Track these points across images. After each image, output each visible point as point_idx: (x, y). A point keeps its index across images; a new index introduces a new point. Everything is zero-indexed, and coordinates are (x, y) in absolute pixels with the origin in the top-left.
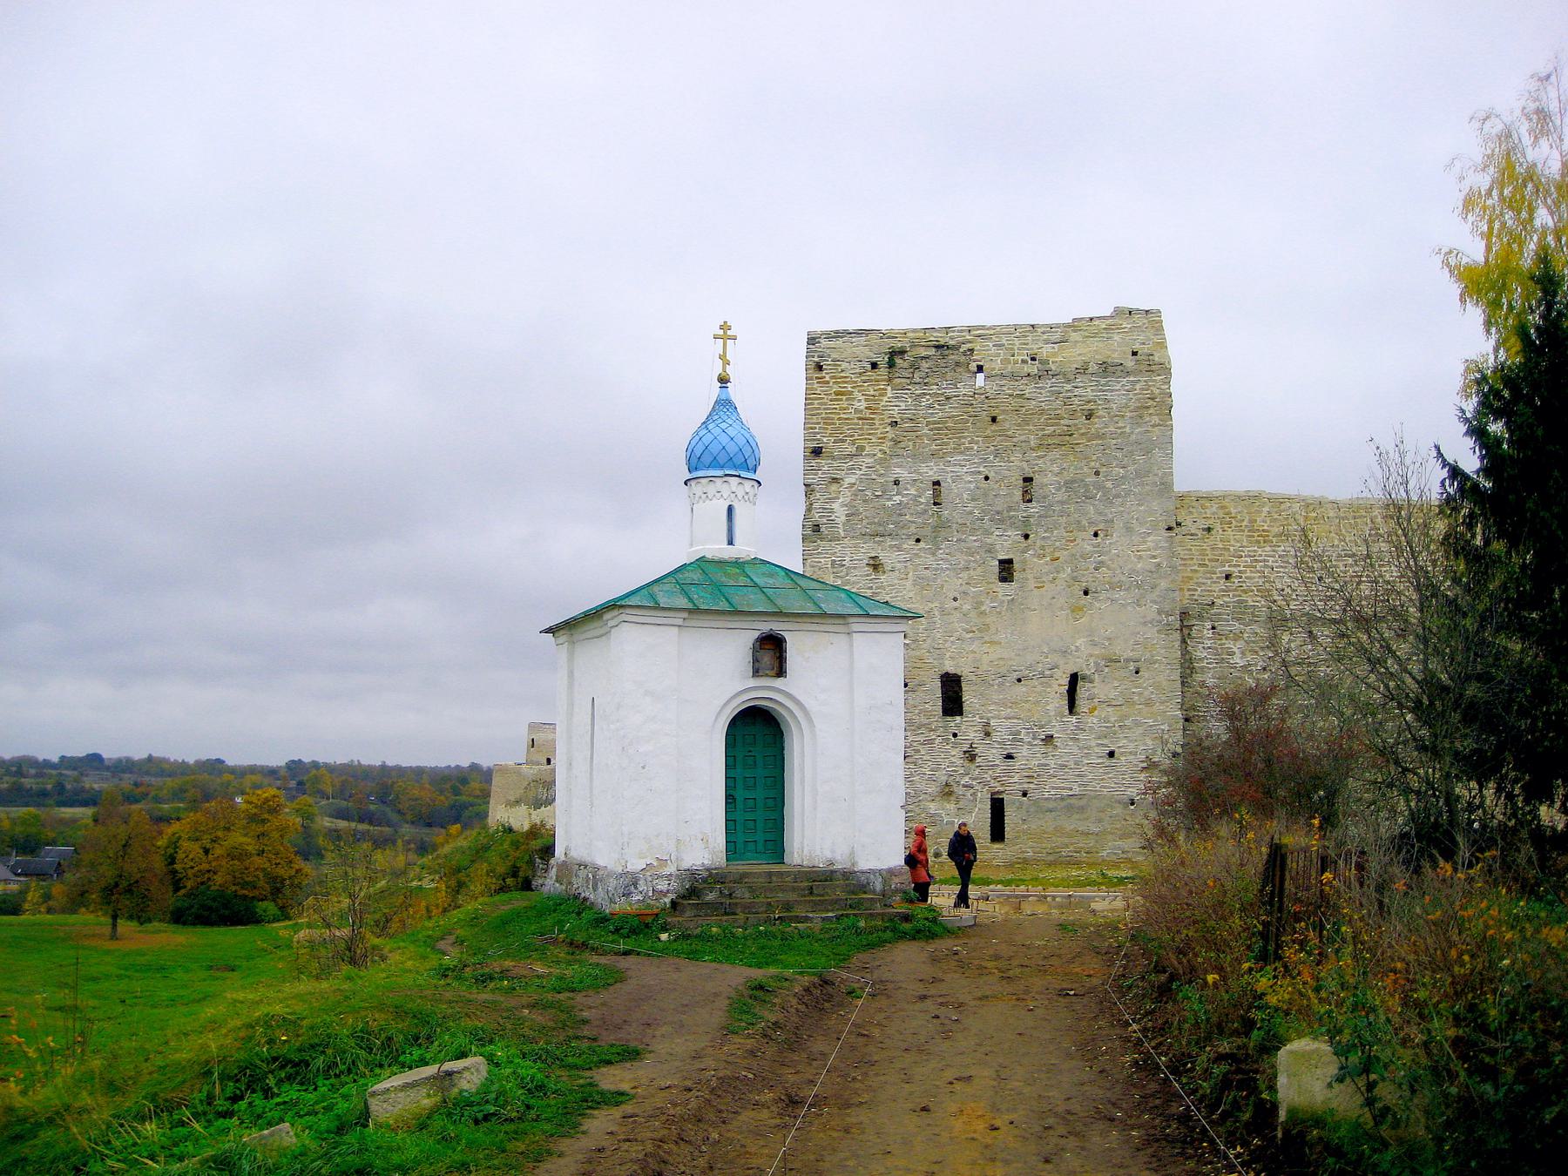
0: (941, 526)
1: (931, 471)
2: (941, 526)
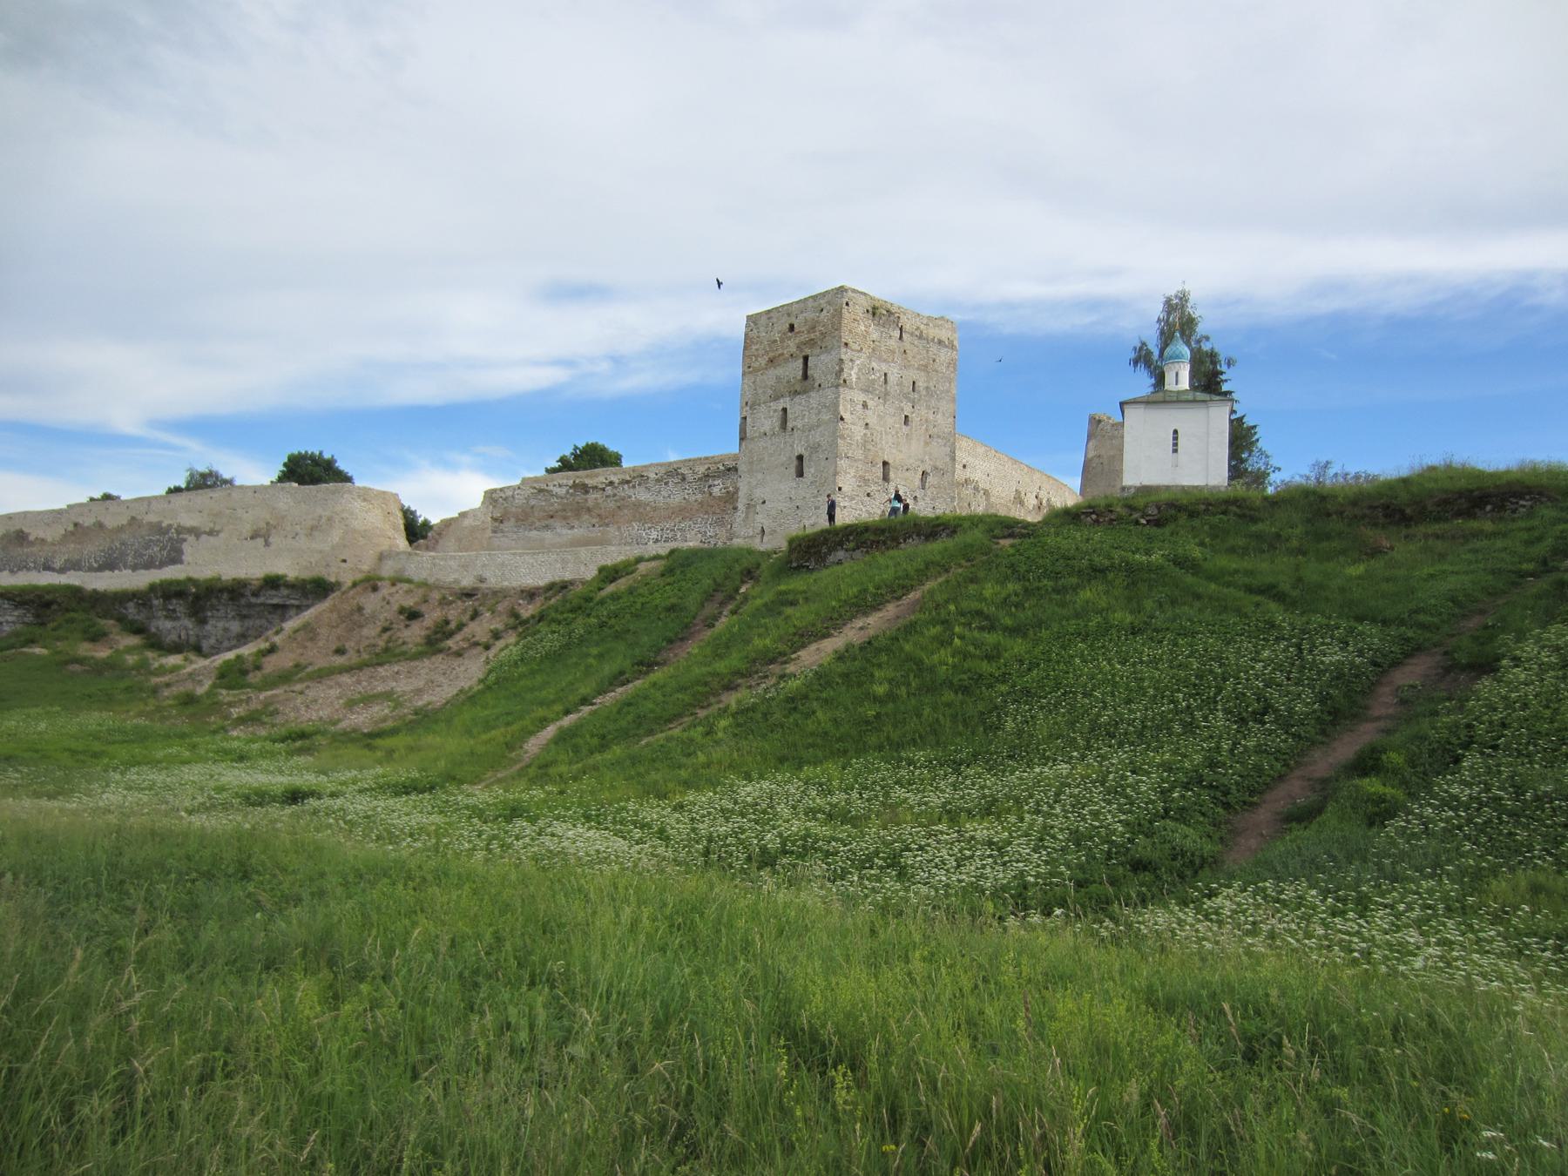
0: (887, 394)
1: (884, 367)
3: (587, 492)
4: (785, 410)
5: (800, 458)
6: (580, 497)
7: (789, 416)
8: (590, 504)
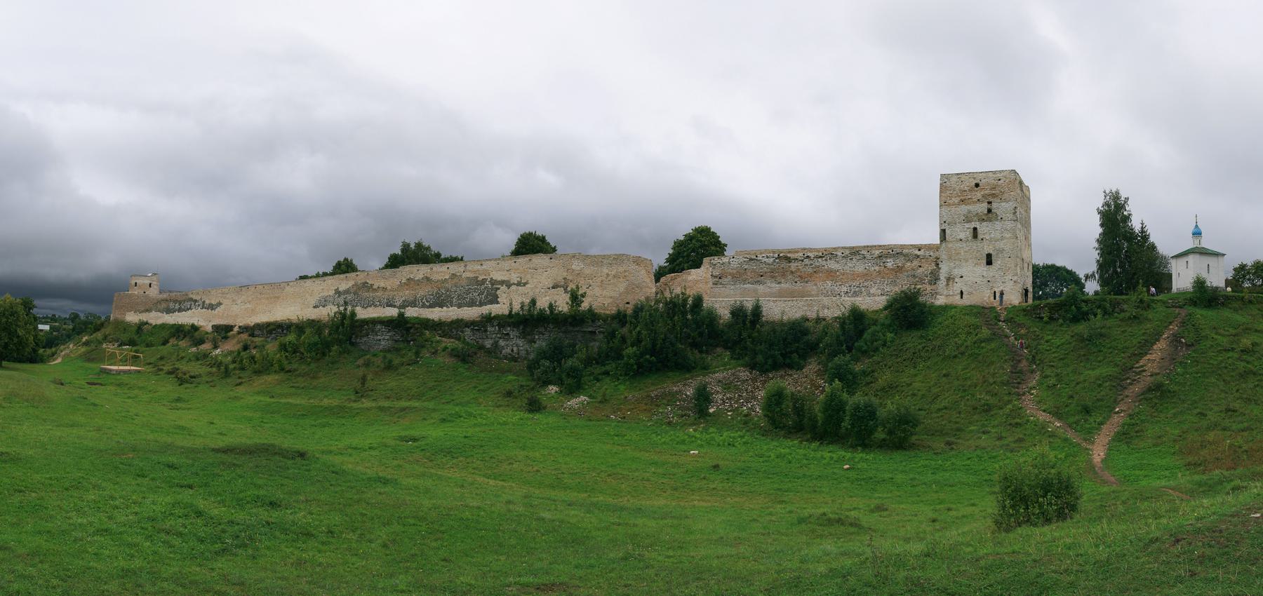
4: (975, 229)
5: (989, 256)
6: (784, 264)
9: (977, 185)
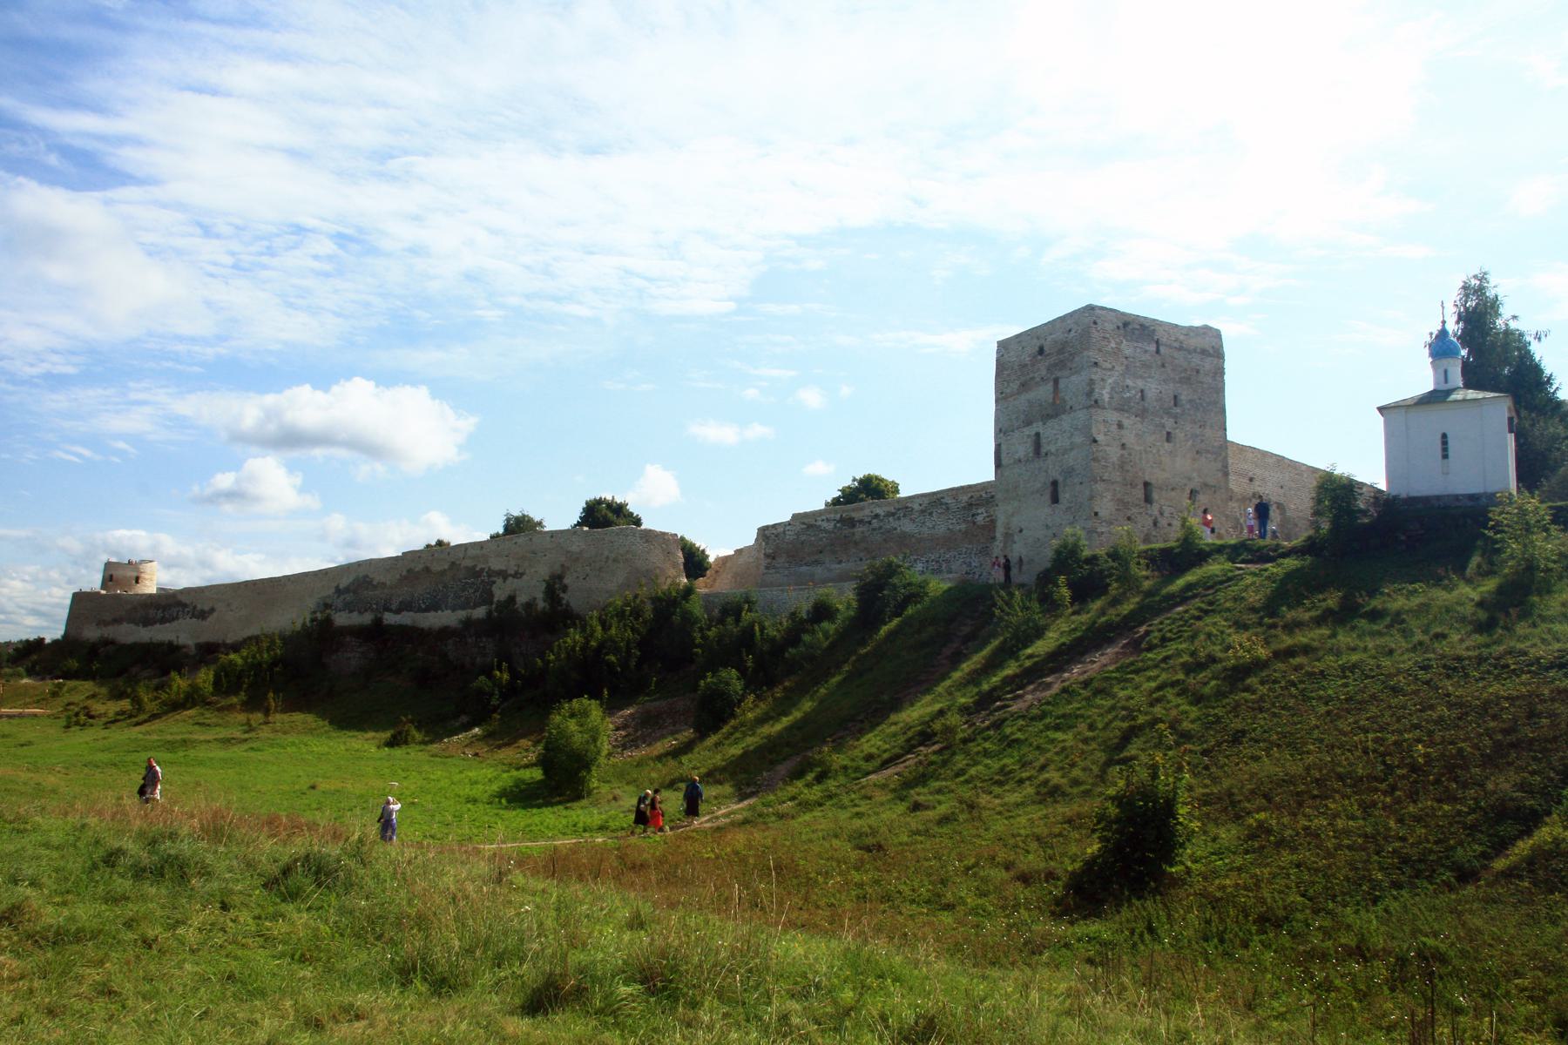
1: (1140, 384)
2: (1145, 410)
3: (854, 526)
4: (1038, 435)
6: (847, 531)
7: (1043, 441)
8: (857, 537)
9: (1041, 351)
